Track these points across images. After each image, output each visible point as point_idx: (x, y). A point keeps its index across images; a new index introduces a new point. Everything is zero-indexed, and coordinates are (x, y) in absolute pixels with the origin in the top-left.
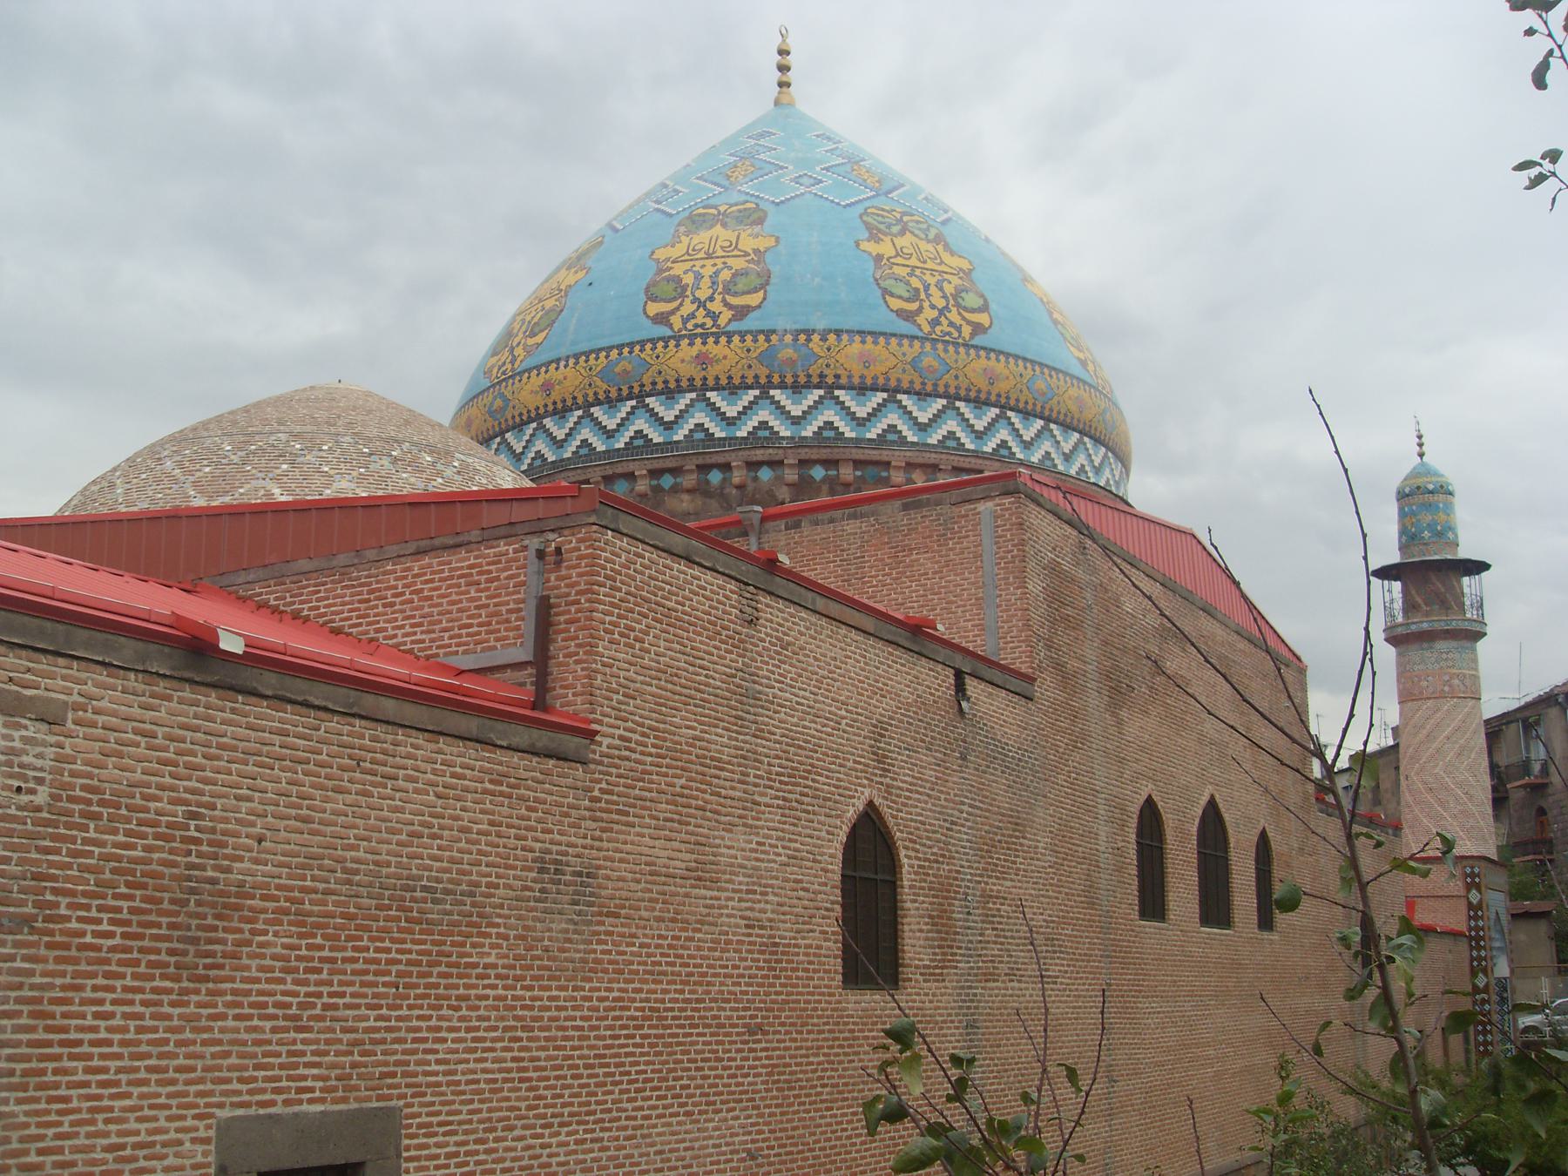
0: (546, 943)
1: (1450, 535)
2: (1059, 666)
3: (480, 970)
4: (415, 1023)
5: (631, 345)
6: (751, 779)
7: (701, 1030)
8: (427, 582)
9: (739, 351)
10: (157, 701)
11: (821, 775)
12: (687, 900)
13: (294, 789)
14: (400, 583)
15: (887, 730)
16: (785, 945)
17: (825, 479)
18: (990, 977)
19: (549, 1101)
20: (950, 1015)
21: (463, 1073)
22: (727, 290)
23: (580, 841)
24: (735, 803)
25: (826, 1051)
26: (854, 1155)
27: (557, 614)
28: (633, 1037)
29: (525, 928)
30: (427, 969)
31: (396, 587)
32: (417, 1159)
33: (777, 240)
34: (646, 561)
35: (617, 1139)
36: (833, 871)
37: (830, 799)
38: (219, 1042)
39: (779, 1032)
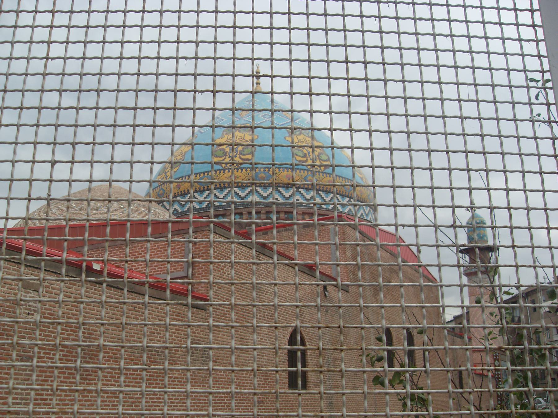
1: (485, 238)
3: (173, 379)
10: (71, 286)
13: (114, 316)
14: (140, 250)
22: (241, 154)
23: (204, 336)
28: (221, 403)
31: (139, 252)
38: (90, 401)
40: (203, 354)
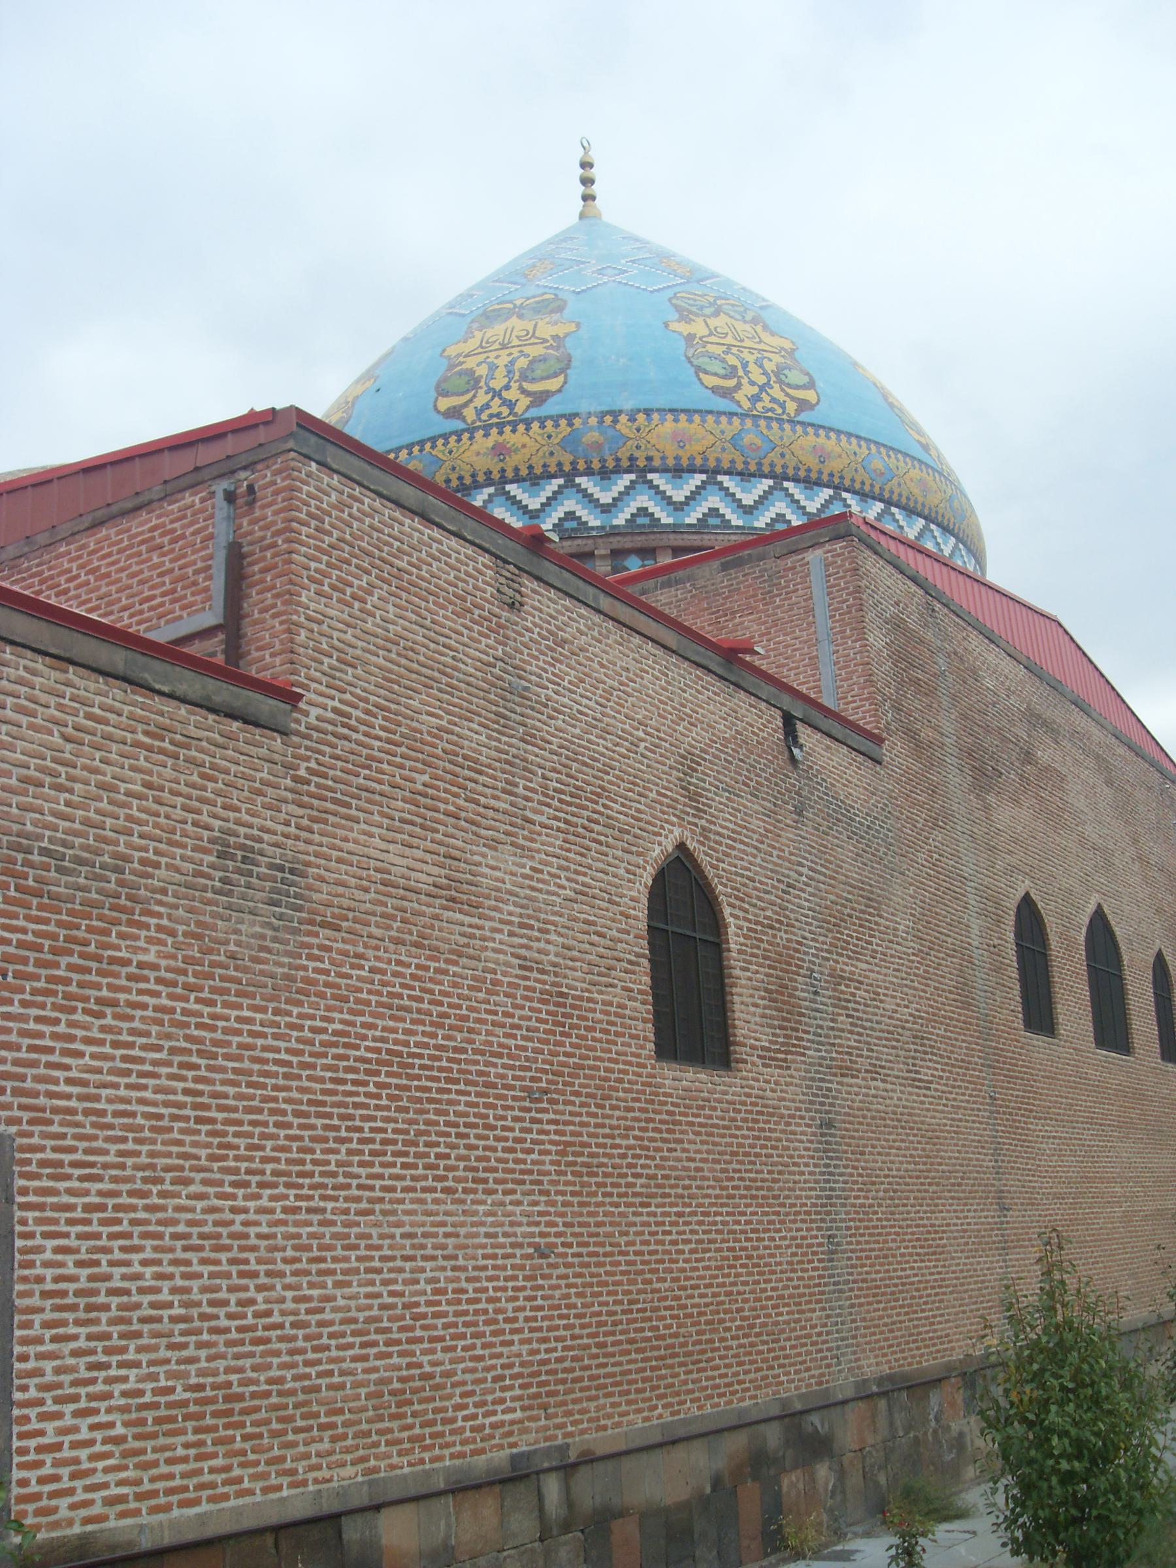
0: (232, 947)
2: (911, 735)
3: (132, 969)
4: (32, 1026)
5: (422, 443)
6: (520, 791)
7: (462, 1087)
8: (104, 557)
9: (539, 438)
11: (615, 802)
12: (436, 923)
14: (74, 565)
15: (699, 764)
16: (574, 997)
18: (847, 1071)
19: (242, 1152)
20: (798, 1109)
21: (110, 1101)
24: (500, 816)
25: (637, 1133)
26: (681, 1264)
27: (251, 564)
28: (365, 1084)
29: (199, 924)
30: (50, 957)
31: (70, 571)
32: (41, 1207)
33: (578, 325)
34: (366, 508)
35: (346, 1212)
36: (636, 918)
37: (628, 833)
39: (573, 1104)
40: (273, 890)
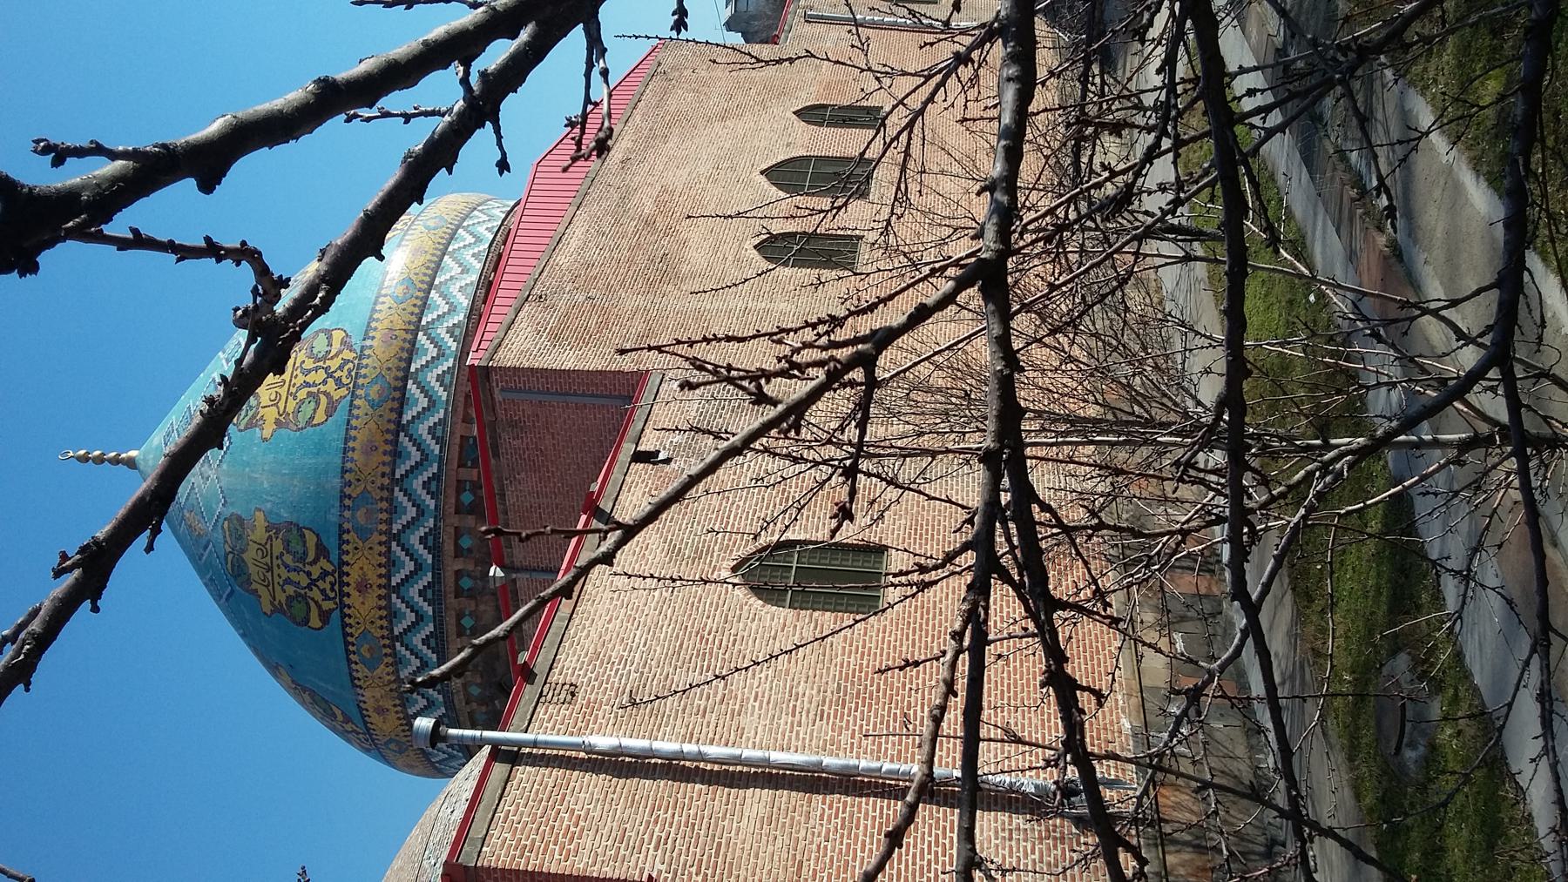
5: (347, 644)
6: (703, 703)
9: (356, 557)
17: (473, 492)
24: (721, 722)
